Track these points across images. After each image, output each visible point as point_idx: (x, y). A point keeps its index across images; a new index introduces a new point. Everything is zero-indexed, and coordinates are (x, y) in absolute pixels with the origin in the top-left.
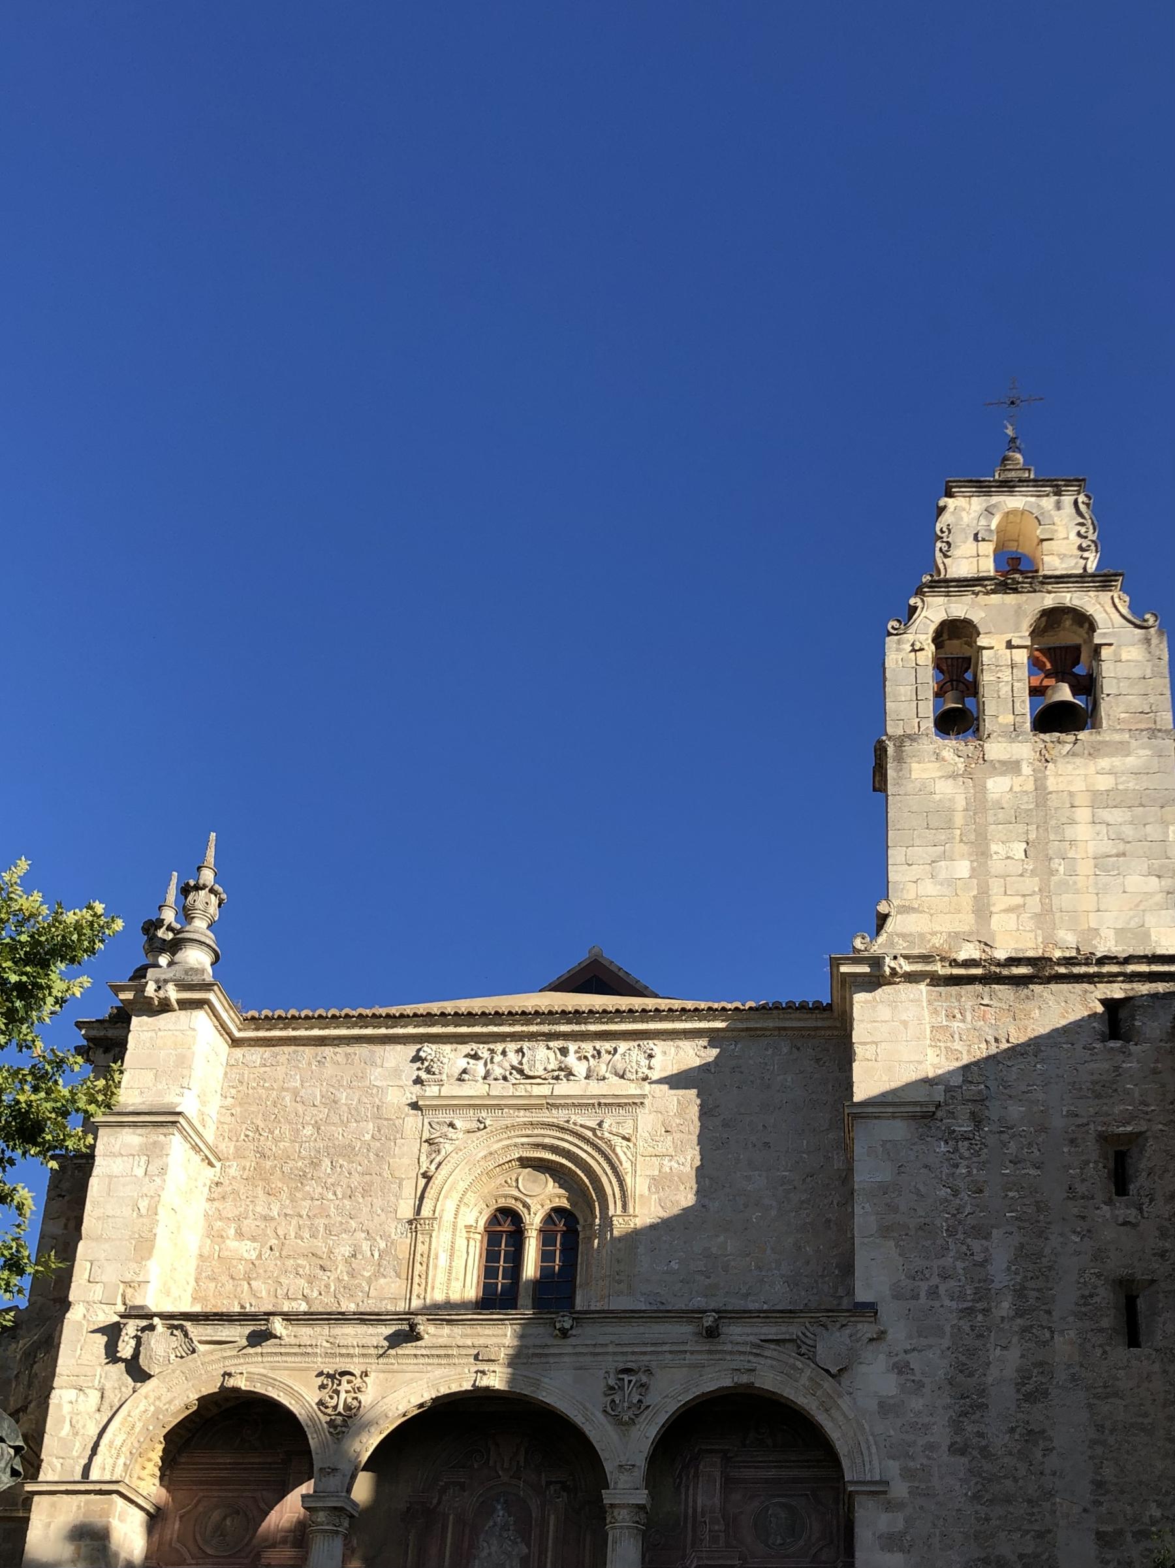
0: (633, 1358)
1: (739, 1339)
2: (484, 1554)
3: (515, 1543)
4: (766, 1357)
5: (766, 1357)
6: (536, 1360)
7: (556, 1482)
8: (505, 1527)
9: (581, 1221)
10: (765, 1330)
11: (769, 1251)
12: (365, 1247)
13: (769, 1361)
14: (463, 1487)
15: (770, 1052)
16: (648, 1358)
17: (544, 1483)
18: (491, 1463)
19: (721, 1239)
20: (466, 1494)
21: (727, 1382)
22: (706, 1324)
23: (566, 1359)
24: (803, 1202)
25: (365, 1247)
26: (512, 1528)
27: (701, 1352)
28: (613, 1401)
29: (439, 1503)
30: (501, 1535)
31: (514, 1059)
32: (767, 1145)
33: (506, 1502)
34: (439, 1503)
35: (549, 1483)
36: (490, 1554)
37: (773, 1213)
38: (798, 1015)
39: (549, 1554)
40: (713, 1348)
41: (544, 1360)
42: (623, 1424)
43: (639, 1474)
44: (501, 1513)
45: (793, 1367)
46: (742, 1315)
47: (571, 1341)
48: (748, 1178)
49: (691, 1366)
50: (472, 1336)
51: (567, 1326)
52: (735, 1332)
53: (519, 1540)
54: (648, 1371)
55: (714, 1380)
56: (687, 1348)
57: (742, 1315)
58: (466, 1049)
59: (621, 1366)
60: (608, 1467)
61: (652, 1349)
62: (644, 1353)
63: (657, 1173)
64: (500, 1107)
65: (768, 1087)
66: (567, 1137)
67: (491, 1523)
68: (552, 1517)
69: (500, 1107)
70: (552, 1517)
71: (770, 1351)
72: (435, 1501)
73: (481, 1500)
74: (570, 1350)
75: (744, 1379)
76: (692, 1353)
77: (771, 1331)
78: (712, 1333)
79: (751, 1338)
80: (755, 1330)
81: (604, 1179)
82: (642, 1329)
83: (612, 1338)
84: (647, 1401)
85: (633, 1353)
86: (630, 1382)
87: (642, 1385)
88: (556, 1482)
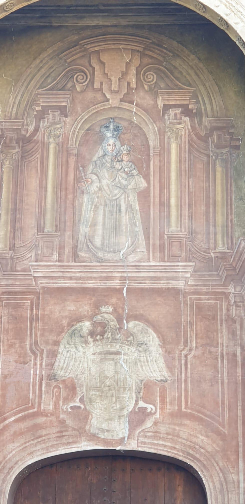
2: (94, 188)
3: (130, 175)
7: (175, 106)
8: (117, 158)
14: (63, 111)
17: (161, 107)
20: (68, 120)
26: (125, 158)
29: (36, 130)
30: (113, 167)
33: (117, 129)
34: (36, 130)
35: (167, 107)
36: (100, 189)
39: (173, 187)
44: (111, 141)
53: (135, 172)
67: (101, 153)
68: (174, 147)
70: (174, 147)
72: (31, 128)
73: (87, 127)
88: (175, 106)
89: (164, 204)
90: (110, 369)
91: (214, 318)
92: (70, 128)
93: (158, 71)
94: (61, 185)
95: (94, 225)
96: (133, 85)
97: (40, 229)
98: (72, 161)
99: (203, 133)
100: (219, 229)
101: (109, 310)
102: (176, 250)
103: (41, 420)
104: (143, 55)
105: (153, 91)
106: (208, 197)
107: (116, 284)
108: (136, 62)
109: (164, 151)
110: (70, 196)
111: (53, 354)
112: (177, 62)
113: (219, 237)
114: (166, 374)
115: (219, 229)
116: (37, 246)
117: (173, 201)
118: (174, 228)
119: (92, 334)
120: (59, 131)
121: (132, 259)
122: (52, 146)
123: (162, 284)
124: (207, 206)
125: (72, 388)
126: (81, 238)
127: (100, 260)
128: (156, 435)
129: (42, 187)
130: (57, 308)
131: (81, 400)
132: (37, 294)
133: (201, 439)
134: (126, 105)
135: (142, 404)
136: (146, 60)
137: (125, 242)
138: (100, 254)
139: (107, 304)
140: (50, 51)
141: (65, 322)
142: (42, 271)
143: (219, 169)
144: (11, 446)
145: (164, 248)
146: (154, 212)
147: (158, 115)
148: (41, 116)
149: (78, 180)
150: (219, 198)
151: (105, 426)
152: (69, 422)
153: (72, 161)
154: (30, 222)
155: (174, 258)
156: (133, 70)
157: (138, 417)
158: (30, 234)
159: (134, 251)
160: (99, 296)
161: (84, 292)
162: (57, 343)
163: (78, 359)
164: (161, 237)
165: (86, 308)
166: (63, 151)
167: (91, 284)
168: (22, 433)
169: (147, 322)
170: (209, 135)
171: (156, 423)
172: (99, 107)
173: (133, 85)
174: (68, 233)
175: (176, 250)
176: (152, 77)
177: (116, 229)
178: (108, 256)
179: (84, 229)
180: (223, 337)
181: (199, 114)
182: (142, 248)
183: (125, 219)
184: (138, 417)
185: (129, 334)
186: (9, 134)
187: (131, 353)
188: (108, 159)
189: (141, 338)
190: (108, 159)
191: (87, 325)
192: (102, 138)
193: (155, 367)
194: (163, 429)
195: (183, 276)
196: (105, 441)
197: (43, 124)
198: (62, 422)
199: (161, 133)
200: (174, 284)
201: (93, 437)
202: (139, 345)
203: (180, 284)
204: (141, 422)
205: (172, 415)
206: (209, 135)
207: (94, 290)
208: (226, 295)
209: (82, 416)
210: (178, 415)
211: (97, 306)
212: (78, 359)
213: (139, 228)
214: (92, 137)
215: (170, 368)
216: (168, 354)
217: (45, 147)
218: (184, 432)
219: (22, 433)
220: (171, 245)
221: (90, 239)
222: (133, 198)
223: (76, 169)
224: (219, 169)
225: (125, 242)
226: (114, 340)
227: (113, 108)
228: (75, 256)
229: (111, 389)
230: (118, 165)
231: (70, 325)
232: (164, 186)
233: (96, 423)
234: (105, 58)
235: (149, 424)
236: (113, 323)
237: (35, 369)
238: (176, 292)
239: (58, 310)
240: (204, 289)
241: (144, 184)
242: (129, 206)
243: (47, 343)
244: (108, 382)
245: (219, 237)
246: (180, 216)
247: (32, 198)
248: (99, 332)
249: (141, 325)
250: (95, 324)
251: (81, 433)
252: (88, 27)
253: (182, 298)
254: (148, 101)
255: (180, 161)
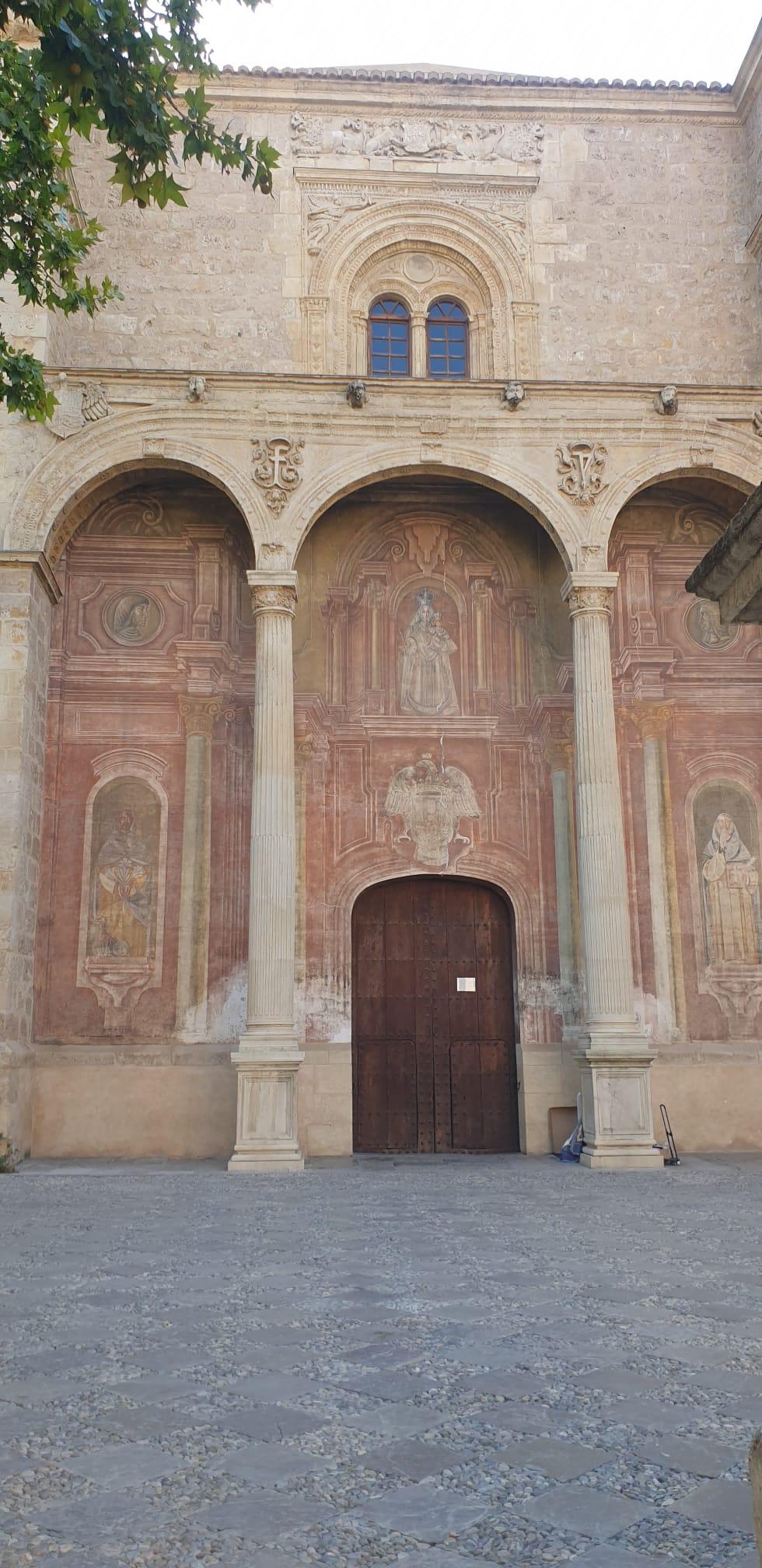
0: (582, 435)
1: (697, 417)
2: (413, 649)
3: (442, 639)
4: (724, 438)
5: (724, 438)
6: (481, 435)
8: (431, 623)
9: (472, 312)
10: (722, 408)
11: (675, 346)
12: (252, 324)
13: (728, 443)
14: (383, 580)
15: (661, 139)
16: (600, 435)
17: (467, 578)
18: (411, 557)
19: (626, 331)
21: (685, 463)
22: (666, 398)
23: (514, 435)
24: (706, 296)
25: (252, 324)
27: (655, 430)
28: (571, 480)
31: (391, 134)
32: (664, 236)
33: (430, 597)
35: (472, 578)
37: (677, 306)
38: (693, 97)
40: (669, 426)
41: (490, 435)
42: (584, 503)
43: (603, 556)
45: (753, 449)
46: (699, 390)
47: (518, 414)
48: (649, 270)
49: (647, 446)
50: (412, 406)
51: (520, 396)
52: (690, 409)
54: (602, 449)
55: (672, 460)
56: (642, 425)
57: (699, 390)
58: (340, 121)
59: (575, 443)
60: (571, 549)
61: (606, 425)
62: (597, 430)
63: (552, 261)
64: (383, 184)
65: (663, 175)
66: (457, 219)
68: (479, 614)
69: (383, 184)
70: (479, 614)
71: (727, 431)
72: (356, 595)
74: (518, 424)
75: (703, 460)
76: (647, 431)
77: (730, 410)
78: (669, 408)
79: (706, 417)
80: (712, 408)
81: (499, 266)
82: (593, 404)
83: (563, 412)
84: (605, 480)
85: (586, 430)
86: (586, 459)
87: (598, 464)
89: (472, 666)
90: (432, 810)
91: (517, 764)
92: (388, 596)
93: (464, 546)
94: (384, 648)
95: (413, 682)
96: (443, 557)
97: (368, 685)
98: (392, 626)
99: (504, 602)
100: (519, 687)
101: (430, 754)
102: (483, 706)
103: (376, 850)
104: (450, 531)
105: (460, 563)
106: (509, 659)
107: (433, 734)
108: (445, 536)
109: (471, 619)
110: (392, 658)
111: (384, 794)
112: (480, 538)
113: (519, 694)
114: (479, 812)
115: (519, 687)
116: (366, 701)
117: (479, 663)
118: (481, 686)
119: (415, 777)
120: (380, 597)
121: (446, 713)
122: (375, 612)
123: (473, 734)
124: (509, 667)
125: (400, 822)
126: (403, 694)
127: (420, 714)
128: (471, 862)
129: (368, 649)
130: (385, 755)
131: (409, 834)
132: (367, 742)
133: (509, 865)
134: (437, 576)
135: (458, 836)
136: (453, 535)
137: (440, 697)
138: (420, 709)
139: (426, 752)
140: (370, 524)
141: (392, 767)
142: (371, 723)
143: (518, 635)
144: (352, 872)
145: (473, 704)
146: (464, 672)
147: (465, 586)
148: (364, 583)
149: (398, 642)
150: (518, 660)
151: (429, 855)
152: (399, 852)
153: (392, 626)
154: (359, 679)
155: (481, 712)
156: (442, 543)
157: (456, 847)
158: (360, 690)
159: (448, 706)
160: (420, 744)
161: (407, 741)
162: (387, 785)
163: (405, 799)
164: (471, 694)
165: (409, 755)
166: (384, 615)
167: (413, 734)
168: (360, 861)
169: (462, 767)
170: (509, 604)
171: (471, 852)
172: (414, 577)
173: (443, 557)
174: (392, 690)
175: (483, 706)
176: (459, 551)
177: (432, 687)
178: (427, 710)
179: (405, 687)
180: (525, 781)
181: (500, 585)
182: (455, 703)
183: (439, 677)
184: (456, 847)
185: (446, 777)
186: (337, 600)
187: (448, 793)
188: (423, 624)
189: (456, 781)
190: (423, 624)
191: (411, 770)
192: (418, 606)
193: (469, 806)
194: (477, 857)
195: (490, 728)
196: (430, 868)
197: (367, 591)
198: (394, 851)
199: (468, 602)
200: (482, 734)
201: (420, 864)
202: (455, 787)
203: (487, 735)
204: (459, 852)
205: (484, 845)
206: (509, 604)
207: (415, 739)
208: (526, 744)
209: (410, 846)
210: (488, 846)
211: (419, 754)
212: (405, 799)
213: (452, 686)
214: (409, 605)
215: (481, 806)
216: (480, 794)
217: (369, 613)
218: (495, 860)
219: (360, 861)
220: (479, 701)
221: (410, 695)
222: (445, 659)
223: (397, 632)
224: (518, 635)
225: (440, 697)
226: (434, 782)
227: (425, 578)
228: (399, 711)
229: (432, 824)
230: (432, 630)
231: (397, 770)
232: (472, 649)
233: (421, 853)
234: (417, 531)
235: (465, 853)
236: (433, 768)
237: (368, 808)
238: (485, 741)
239: (387, 757)
240: (507, 739)
241: (455, 647)
242: (442, 666)
243: (378, 784)
244: (430, 818)
245: (519, 694)
246: (486, 676)
247: (360, 658)
248: (421, 775)
249: (456, 770)
250: (417, 769)
251: (410, 861)
252: (402, 504)
253: (489, 746)
254: (456, 572)
255: (484, 627)
